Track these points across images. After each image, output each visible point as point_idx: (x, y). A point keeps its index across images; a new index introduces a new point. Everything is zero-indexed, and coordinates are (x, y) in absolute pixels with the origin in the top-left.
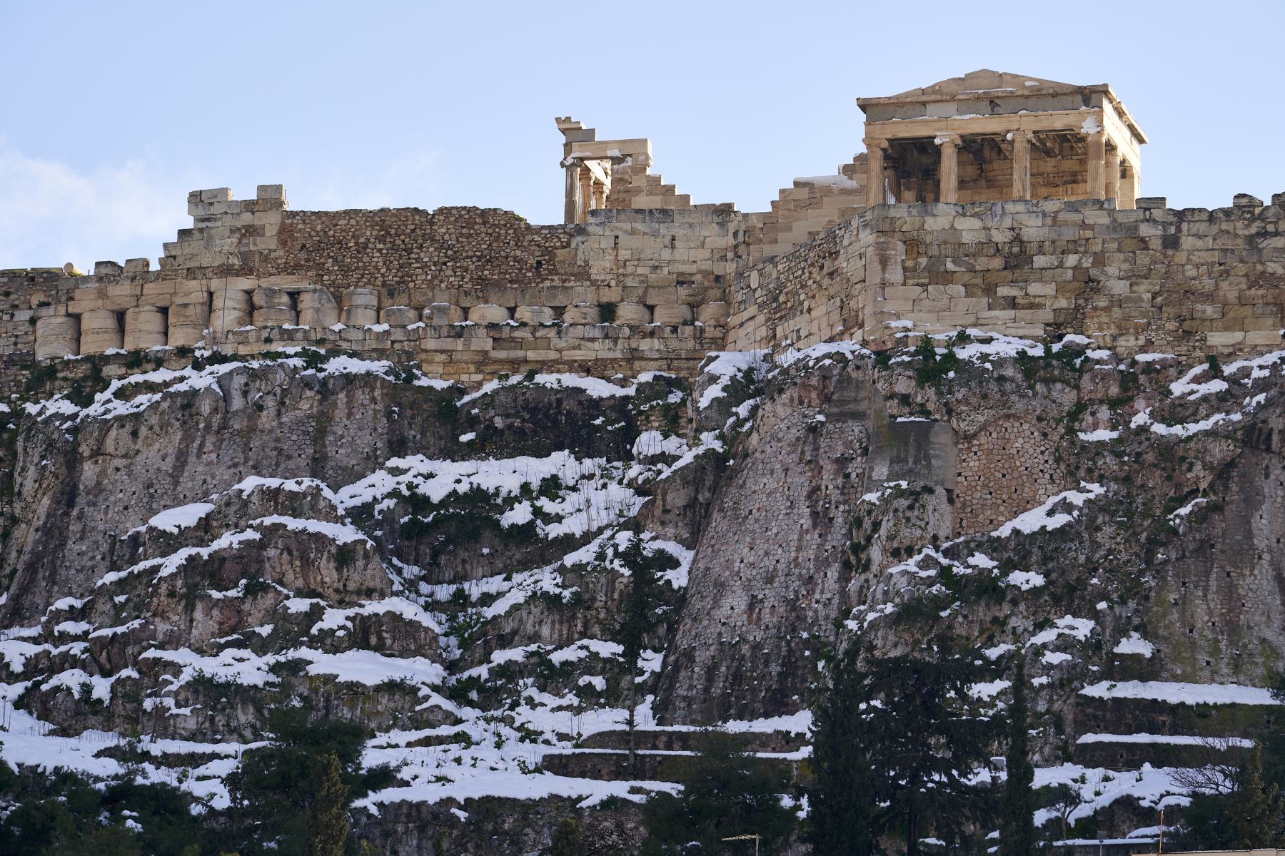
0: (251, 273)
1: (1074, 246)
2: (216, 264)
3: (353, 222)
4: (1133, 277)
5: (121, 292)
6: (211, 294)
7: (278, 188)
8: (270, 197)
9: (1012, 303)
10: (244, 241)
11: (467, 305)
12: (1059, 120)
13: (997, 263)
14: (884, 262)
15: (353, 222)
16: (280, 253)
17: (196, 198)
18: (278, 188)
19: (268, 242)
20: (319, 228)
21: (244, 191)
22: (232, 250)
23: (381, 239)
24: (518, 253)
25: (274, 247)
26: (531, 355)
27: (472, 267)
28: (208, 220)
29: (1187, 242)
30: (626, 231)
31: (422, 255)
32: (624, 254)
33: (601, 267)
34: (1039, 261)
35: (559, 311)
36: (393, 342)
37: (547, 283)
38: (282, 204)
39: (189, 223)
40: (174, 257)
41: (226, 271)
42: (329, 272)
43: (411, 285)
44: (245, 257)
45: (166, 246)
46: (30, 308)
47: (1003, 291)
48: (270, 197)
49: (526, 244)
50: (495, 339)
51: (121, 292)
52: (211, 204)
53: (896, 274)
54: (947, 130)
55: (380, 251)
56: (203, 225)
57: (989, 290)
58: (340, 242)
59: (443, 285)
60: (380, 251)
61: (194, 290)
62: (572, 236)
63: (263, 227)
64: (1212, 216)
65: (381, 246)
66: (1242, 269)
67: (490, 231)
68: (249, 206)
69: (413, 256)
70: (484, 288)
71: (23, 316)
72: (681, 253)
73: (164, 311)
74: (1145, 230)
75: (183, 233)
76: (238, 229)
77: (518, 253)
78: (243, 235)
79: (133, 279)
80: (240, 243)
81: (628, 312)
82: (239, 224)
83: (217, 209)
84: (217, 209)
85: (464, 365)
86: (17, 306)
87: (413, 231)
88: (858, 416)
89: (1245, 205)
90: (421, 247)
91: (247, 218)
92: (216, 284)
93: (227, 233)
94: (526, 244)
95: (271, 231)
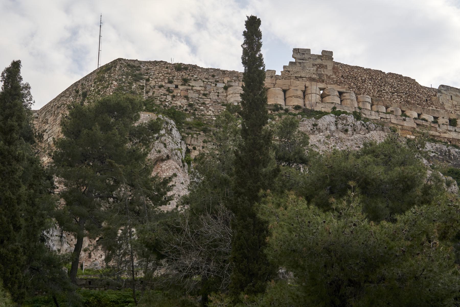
0: (323, 82)
2: (308, 77)
3: (359, 71)
6: (306, 87)
7: (331, 53)
8: (327, 55)
10: (319, 70)
11: (404, 110)
15: (359, 71)
16: (334, 76)
17: (296, 51)
18: (331, 53)
19: (329, 72)
20: (347, 70)
21: (316, 51)
22: (314, 72)
23: (371, 79)
24: (419, 95)
25: (331, 74)
26: (431, 132)
27: (404, 96)
28: (303, 60)
30: (454, 95)
31: (385, 88)
32: (455, 103)
33: (448, 105)
36: (381, 118)
37: (431, 108)
38: (333, 59)
39: (294, 60)
40: (289, 71)
41: (312, 80)
42: (352, 88)
43: (383, 98)
44: (320, 75)
45: (284, 67)
46: (224, 83)
48: (327, 55)
49: (421, 92)
50: (417, 124)
52: (303, 54)
55: (370, 83)
56: (301, 61)
58: (355, 77)
59: (394, 101)
60: (370, 83)
61: (300, 85)
62: (436, 93)
63: (326, 66)
65: (370, 82)
67: (408, 85)
68: (319, 57)
69: (382, 88)
71: (221, 85)
73: (285, 91)
75: (291, 63)
76: (316, 65)
77: (419, 95)
78: (318, 68)
79: (272, 77)
80: (317, 70)
82: (316, 63)
83: (306, 56)
84: (306, 56)
85: (407, 132)
86: (218, 81)
87: (381, 79)
90: (384, 85)
91: (319, 61)
92: (308, 84)
93: (312, 66)
94: (421, 92)
95: (330, 68)
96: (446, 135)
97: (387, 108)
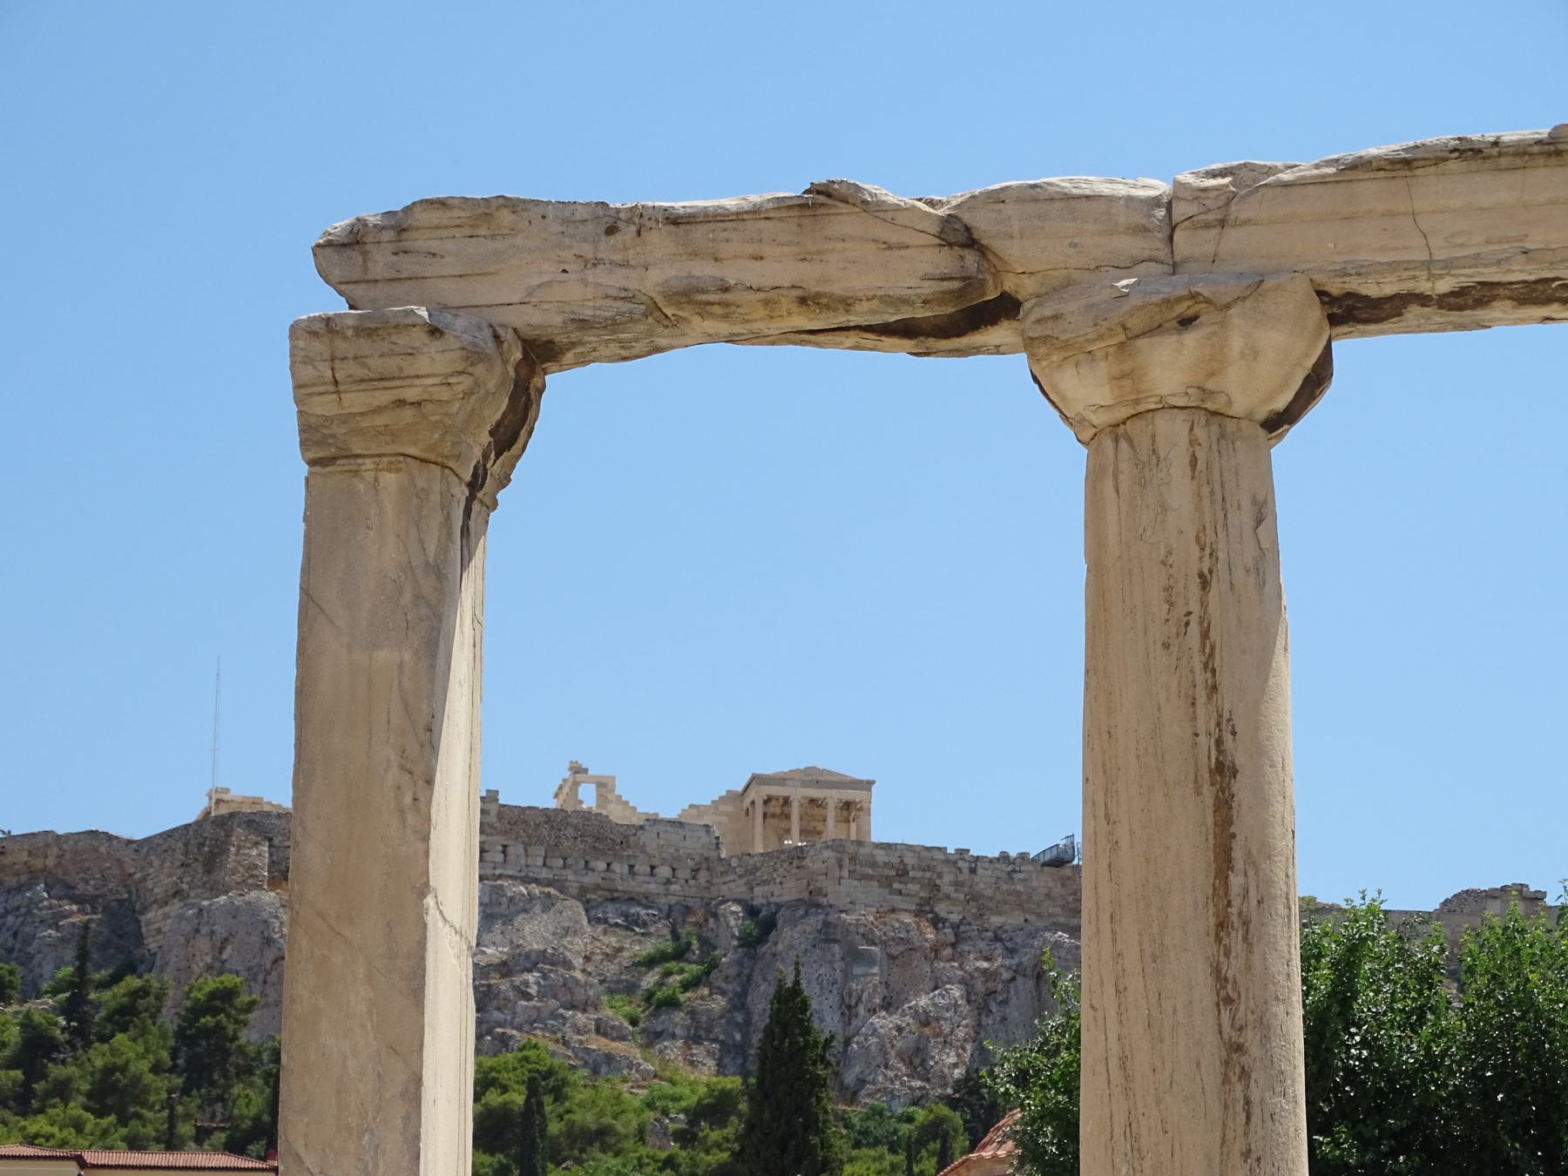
1: (928, 868)
4: (957, 884)
9: (900, 893)
12: (851, 795)
13: (893, 873)
14: (841, 867)
29: (980, 871)
32: (662, 842)
34: (911, 874)
35: (631, 867)
47: (896, 886)
53: (845, 873)
54: (798, 794)
57: (890, 886)
64: (991, 861)
66: (1005, 887)
72: (688, 843)
74: (961, 864)
81: (664, 871)
88: (835, 941)
89: (1004, 857)
96: (642, 890)
97: (565, 859)
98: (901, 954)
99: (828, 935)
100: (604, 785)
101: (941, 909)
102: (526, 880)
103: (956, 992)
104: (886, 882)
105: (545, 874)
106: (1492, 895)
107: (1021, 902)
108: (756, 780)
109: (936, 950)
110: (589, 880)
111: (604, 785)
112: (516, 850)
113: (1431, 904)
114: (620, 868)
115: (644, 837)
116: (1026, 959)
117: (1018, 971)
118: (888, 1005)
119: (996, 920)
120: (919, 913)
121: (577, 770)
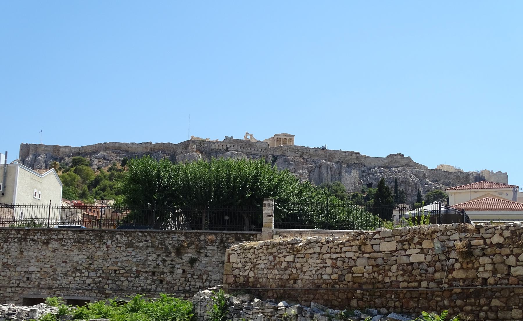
5: (219, 144)
8: (232, 137)
48: (232, 137)
51: (219, 144)
54: (282, 137)
70: (249, 147)
81: (260, 150)
89: (315, 148)
98: (297, 164)
99: (285, 160)
100: (251, 136)
101: (304, 156)
102: (237, 151)
103: (306, 170)
104: (295, 152)
105: (240, 150)
106: (395, 155)
107: (317, 155)
108: (275, 135)
109: (303, 163)
110: (247, 151)
111: (251, 136)
112: (236, 146)
113: (385, 157)
114: (253, 149)
115: (257, 144)
116: (318, 164)
117: (316, 166)
118: (295, 172)
119: (313, 158)
120: (300, 157)
121: (247, 133)
